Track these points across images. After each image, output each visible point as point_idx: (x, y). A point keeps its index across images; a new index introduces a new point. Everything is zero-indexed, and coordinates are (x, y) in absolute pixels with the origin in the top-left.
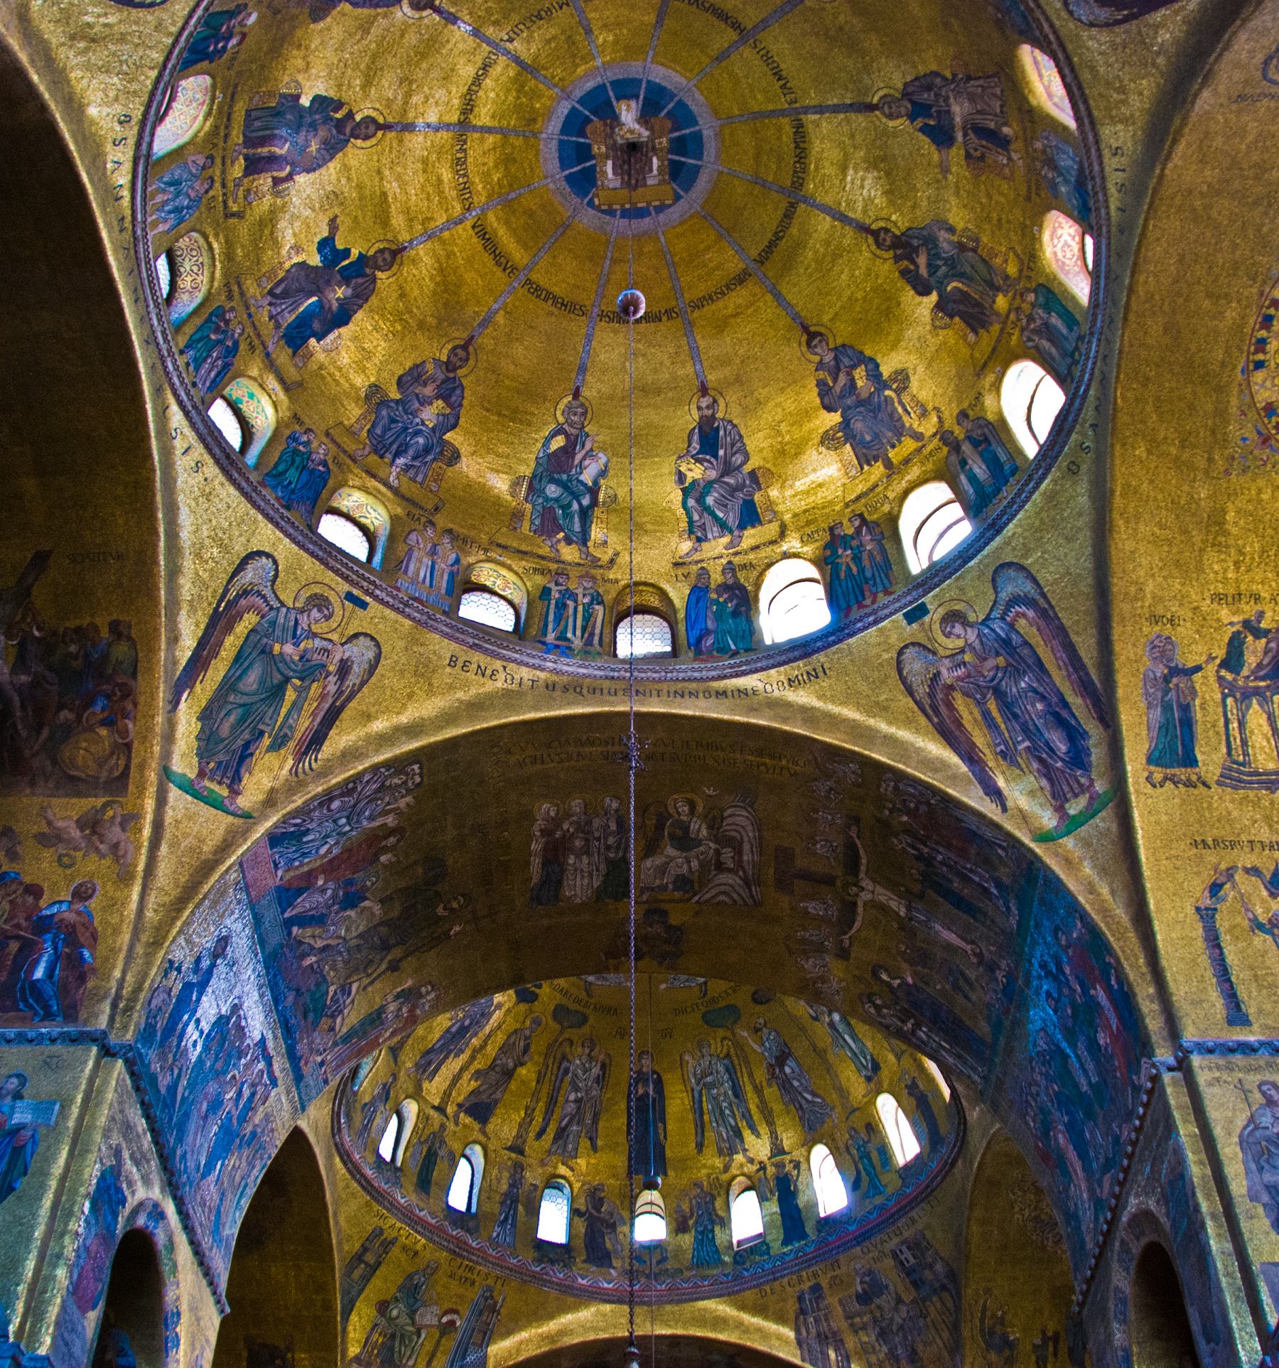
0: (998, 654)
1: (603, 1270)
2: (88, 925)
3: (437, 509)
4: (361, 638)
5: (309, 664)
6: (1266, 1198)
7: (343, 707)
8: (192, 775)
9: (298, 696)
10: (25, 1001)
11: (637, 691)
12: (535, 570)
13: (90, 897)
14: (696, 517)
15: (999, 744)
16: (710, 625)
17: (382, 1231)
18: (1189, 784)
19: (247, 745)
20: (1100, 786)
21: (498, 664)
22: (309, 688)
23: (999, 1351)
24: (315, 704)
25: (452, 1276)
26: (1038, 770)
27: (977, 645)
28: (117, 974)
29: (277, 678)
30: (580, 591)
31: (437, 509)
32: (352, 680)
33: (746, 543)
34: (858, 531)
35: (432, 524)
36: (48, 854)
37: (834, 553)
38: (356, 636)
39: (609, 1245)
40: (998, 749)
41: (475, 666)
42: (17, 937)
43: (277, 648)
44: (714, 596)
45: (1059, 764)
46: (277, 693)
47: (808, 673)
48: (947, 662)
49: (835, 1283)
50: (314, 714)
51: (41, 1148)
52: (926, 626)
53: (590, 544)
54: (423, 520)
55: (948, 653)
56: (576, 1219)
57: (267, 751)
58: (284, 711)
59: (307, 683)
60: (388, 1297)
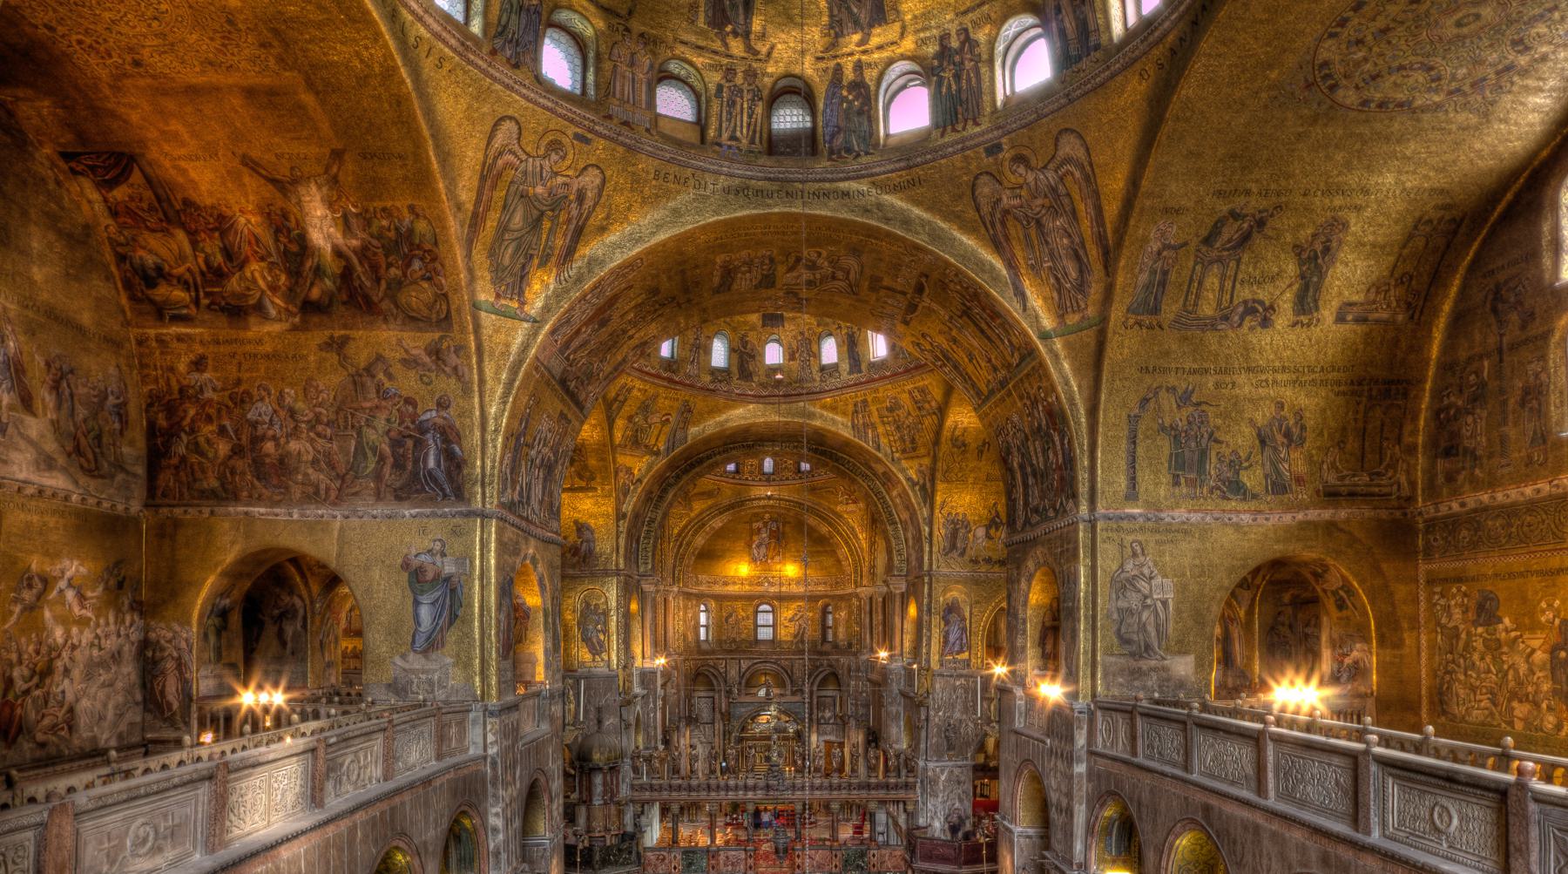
0: (1046, 196)
2: (452, 427)
3: (630, 13)
6: (1115, 616)
7: (584, 224)
8: (492, 299)
10: (428, 484)
11: (787, 193)
12: (710, 65)
13: (448, 406)
14: (836, 12)
16: (842, 124)
18: (1151, 327)
19: (523, 267)
20: (1091, 311)
21: (689, 171)
22: (558, 216)
28: (479, 463)
30: (745, 87)
31: (630, 13)
32: (588, 203)
33: (875, 41)
34: (963, 44)
35: (627, 30)
36: (412, 374)
37: (941, 65)
38: (585, 168)
41: (671, 177)
42: (410, 436)
44: (845, 93)
45: (1068, 286)
46: (535, 224)
48: (1008, 192)
49: (876, 400)
50: (565, 235)
51: (465, 590)
53: (752, 36)
54: (621, 28)
55: (1010, 185)
58: (544, 236)
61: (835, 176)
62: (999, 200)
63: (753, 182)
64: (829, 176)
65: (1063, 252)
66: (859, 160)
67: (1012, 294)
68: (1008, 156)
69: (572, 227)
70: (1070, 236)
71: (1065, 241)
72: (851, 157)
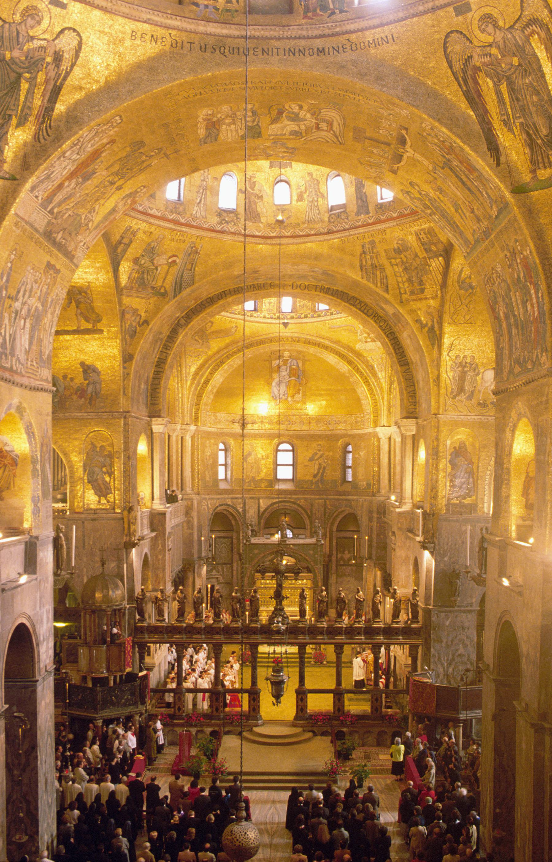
1: (256, 225)
4: (66, 32)
5: (33, 60)
7: (62, 85)
9: (30, 85)
11: (263, 50)
15: (504, 114)
17: (131, 227)
22: (36, 77)
23: (466, 291)
24: (43, 88)
25: (172, 240)
26: (525, 140)
27: (501, 43)
29: (13, 76)
32: (65, 66)
38: (62, 31)
39: (259, 209)
40: (503, 118)
43: (8, 55)
45: (539, 142)
47: (382, 38)
48: (478, 50)
50: (43, 95)
52: (469, 21)
55: (481, 44)
56: (240, 195)
57: (17, 127)
58: (22, 98)
59: (34, 75)
60: (138, 255)
61: (310, 33)
62: (471, 57)
63: (229, 39)
64: (304, 33)
65: (533, 109)
66: (334, 17)
67: (486, 149)
68: (477, 16)
69: (50, 87)
70: (538, 94)
71: (535, 98)
72: (326, 15)
